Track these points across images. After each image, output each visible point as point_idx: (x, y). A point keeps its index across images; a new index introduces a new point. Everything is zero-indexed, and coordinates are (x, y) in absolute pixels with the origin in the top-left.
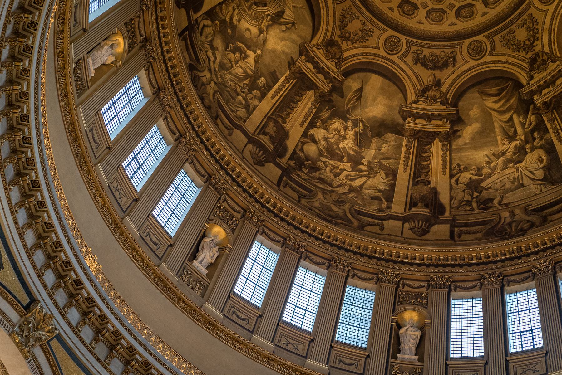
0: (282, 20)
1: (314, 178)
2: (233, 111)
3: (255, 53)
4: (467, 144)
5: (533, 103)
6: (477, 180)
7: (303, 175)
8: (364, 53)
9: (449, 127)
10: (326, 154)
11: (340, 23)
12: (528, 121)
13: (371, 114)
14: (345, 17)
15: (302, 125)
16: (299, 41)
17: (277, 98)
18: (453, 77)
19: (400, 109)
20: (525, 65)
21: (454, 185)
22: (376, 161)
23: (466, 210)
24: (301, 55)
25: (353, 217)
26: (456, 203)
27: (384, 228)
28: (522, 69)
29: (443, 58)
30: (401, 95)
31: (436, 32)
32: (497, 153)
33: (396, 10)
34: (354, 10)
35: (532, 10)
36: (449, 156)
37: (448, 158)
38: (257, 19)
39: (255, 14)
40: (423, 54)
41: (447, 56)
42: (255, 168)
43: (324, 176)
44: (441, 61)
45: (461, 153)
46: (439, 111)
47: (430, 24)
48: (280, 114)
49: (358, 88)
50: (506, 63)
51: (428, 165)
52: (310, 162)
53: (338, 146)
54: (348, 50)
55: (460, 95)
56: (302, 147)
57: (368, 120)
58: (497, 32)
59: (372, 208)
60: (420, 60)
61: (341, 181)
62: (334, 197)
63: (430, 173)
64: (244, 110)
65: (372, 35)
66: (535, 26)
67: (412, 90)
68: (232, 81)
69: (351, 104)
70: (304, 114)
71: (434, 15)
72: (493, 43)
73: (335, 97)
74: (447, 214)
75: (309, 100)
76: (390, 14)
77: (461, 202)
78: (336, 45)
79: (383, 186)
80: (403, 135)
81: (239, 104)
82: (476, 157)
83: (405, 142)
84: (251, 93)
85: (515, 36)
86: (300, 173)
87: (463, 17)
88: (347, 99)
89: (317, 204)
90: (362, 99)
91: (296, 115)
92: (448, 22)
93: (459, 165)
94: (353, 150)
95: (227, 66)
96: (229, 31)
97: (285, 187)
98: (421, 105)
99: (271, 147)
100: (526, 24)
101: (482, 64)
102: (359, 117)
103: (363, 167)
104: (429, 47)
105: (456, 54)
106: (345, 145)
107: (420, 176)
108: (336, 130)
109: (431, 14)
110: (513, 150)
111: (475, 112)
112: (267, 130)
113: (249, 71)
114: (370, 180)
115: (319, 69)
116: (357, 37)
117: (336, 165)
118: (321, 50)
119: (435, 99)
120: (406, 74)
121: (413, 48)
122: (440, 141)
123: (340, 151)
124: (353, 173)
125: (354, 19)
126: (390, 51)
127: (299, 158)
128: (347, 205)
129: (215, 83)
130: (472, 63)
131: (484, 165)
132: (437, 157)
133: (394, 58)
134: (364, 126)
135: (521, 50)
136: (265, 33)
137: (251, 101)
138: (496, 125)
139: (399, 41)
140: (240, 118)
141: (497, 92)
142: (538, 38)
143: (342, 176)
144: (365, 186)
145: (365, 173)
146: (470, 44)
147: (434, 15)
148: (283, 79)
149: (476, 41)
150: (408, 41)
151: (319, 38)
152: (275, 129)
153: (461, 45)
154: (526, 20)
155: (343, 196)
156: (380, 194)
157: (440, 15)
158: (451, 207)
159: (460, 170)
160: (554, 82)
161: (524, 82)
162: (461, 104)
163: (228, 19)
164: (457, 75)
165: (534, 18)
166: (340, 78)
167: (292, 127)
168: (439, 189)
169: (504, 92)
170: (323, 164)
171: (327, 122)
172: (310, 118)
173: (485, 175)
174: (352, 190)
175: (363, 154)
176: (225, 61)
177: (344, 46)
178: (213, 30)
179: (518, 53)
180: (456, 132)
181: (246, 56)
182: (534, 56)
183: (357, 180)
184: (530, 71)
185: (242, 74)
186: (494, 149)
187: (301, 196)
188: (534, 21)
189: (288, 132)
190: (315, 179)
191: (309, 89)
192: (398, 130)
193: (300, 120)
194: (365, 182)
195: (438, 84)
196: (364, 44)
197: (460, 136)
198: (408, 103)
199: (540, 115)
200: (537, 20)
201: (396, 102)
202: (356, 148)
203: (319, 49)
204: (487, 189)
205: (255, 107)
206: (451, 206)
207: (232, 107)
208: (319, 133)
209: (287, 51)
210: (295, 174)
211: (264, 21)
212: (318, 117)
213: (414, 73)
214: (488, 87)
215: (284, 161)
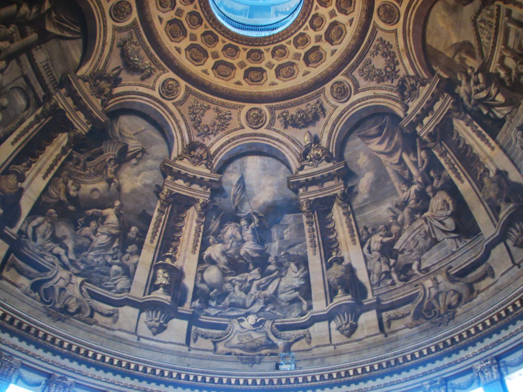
0: (129, 155)
1: (224, 308)
2: (110, 289)
3: (113, 208)
4: (366, 200)
5: (418, 136)
7: (213, 311)
8: (231, 139)
9: (342, 186)
10: (229, 271)
11: (192, 122)
12: (419, 160)
13: (261, 201)
14: (195, 114)
15: (194, 252)
16: (158, 164)
17: (157, 238)
18: (328, 128)
19: (288, 182)
20: (395, 94)
22: (282, 253)
23: (387, 286)
24: (165, 177)
25: (276, 337)
26: (375, 277)
27: (310, 338)
28: (393, 100)
29: (311, 111)
30: (284, 167)
31: (293, 87)
32: (400, 204)
33: (243, 82)
34: (201, 102)
36: (353, 220)
37: (353, 223)
38: (99, 173)
39: (94, 170)
40: (290, 115)
41: (314, 108)
42: (156, 341)
43: (235, 299)
44: (310, 116)
45: (363, 212)
47: (284, 81)
48: (167, 254)
49: (238, 179)
51: (335, 238)
52: (215, 290)
53: (239, 254)
54: (212, 144)
55: (342, 145)
56: (202, 277)
57: (260, 209)
58: (354, 67)
59: (293, 318)
61: (253, 297)
62: (252, 319)
63: (340, 247)
64: (124, 278)
65: (231, 118)
66: (389, 50)
67: (294, 157)
68: (97, 256)
69: (238, 199)
70: (192, 237)
71: (284, 71)
74: (370, 296)
75: (192, 219)
76: (239, 88)
77: (380, 274)
78: (198, 146)
79: (297, 282)
80: (301, 211)
81: (115, 276)
82: (380, 213)
83: (305, 219)
84: (124, 253)
85: (373, 67)
86: (207, 311)
87: (313, 62)
88: (232, 196)
90: (247, 188)
92: (301, 73)
93: (366, 228)
94: (256, 251)
95: (85, 245)
96: (71, 208)
97: (195, 340)
98: (308, 170)
100: (379, 50)
101: (352, 104)
102: (250, 211)
103: (271, 267)
104: (292, 105)
105: (322, 103)
106: (245, 249)
108: (233, 236)
109: (281, 70)
110: (414, 197)
111: (363, 160)
112: (158, 282)
113: (114, 232)
114: (283, 279)
115: (191, 180)
116: (216, 127)
117: (244, 279)
118: (185, 160)
119: (318, 158)
120: (281, 142)
121: (278, 113)
122: (339, 204)
123: (243, 259)
124: (263, 280)
125: (205, 111)
126: (256, 125)
127: (203, 291)
128: (268, 324)
129: (77, 275)
130: (342, 107)
131: (391, 221)
132: (342, 225)
133: (263, 130)
134: (259, 217)
135: (385, 78)
136: (116, 180)
137: (128, 263)
138: (389, 170)
139: (260, 111)
140: (122, 291)
141: (377, 132)
142: (397, 62)
143: (253, 289)
144: (279, 290)
145: (276, 273)
146: (332, 87)
147: (283, 71)
148: (156, 214)
149: (337, 83)
150: (270, 108)
151: (177, 148)
152: (166, 275)
154: (378, 46)
155: (261, 314)
157: (289, 69)
158: (372, 286)
159: (368, 234)
161: (401, 114)
162: (346, 154)
163: (63, 197)
164: (331, 124)
165: (385, 41)
166: (216, 177)
167: (184, 260)
168: (354, 265)
169: (385, 130)
170: (229, 284)
172: (200, 239)
173: (395, 234)
176: (80, 242)
177: (207, 142)
178: (49, 223)
179: (383, 83)
180: (351, 189)
181: (104, 218)
182: (401, 83)
183: (270, 286)
184: (403, 100)
185: (107, 240)
186: (395, 199)
189: (182, 268)
190: (226, 309)
191: (188, 207)
193: (190, 247)
195: (316, 140)
196: (227, 130)
197: (357, 193)
198: (294, 172)
200: (389, 43)
202: (259, 248)
203: (183, 159)
205: (136, 266)
206: (371, 284)
207: (109, 285)
209: (148, 182)
210: (204, 315)
211: (109, 169)
213: (288, 137)
214: (367, 128)
215: (187, 308)
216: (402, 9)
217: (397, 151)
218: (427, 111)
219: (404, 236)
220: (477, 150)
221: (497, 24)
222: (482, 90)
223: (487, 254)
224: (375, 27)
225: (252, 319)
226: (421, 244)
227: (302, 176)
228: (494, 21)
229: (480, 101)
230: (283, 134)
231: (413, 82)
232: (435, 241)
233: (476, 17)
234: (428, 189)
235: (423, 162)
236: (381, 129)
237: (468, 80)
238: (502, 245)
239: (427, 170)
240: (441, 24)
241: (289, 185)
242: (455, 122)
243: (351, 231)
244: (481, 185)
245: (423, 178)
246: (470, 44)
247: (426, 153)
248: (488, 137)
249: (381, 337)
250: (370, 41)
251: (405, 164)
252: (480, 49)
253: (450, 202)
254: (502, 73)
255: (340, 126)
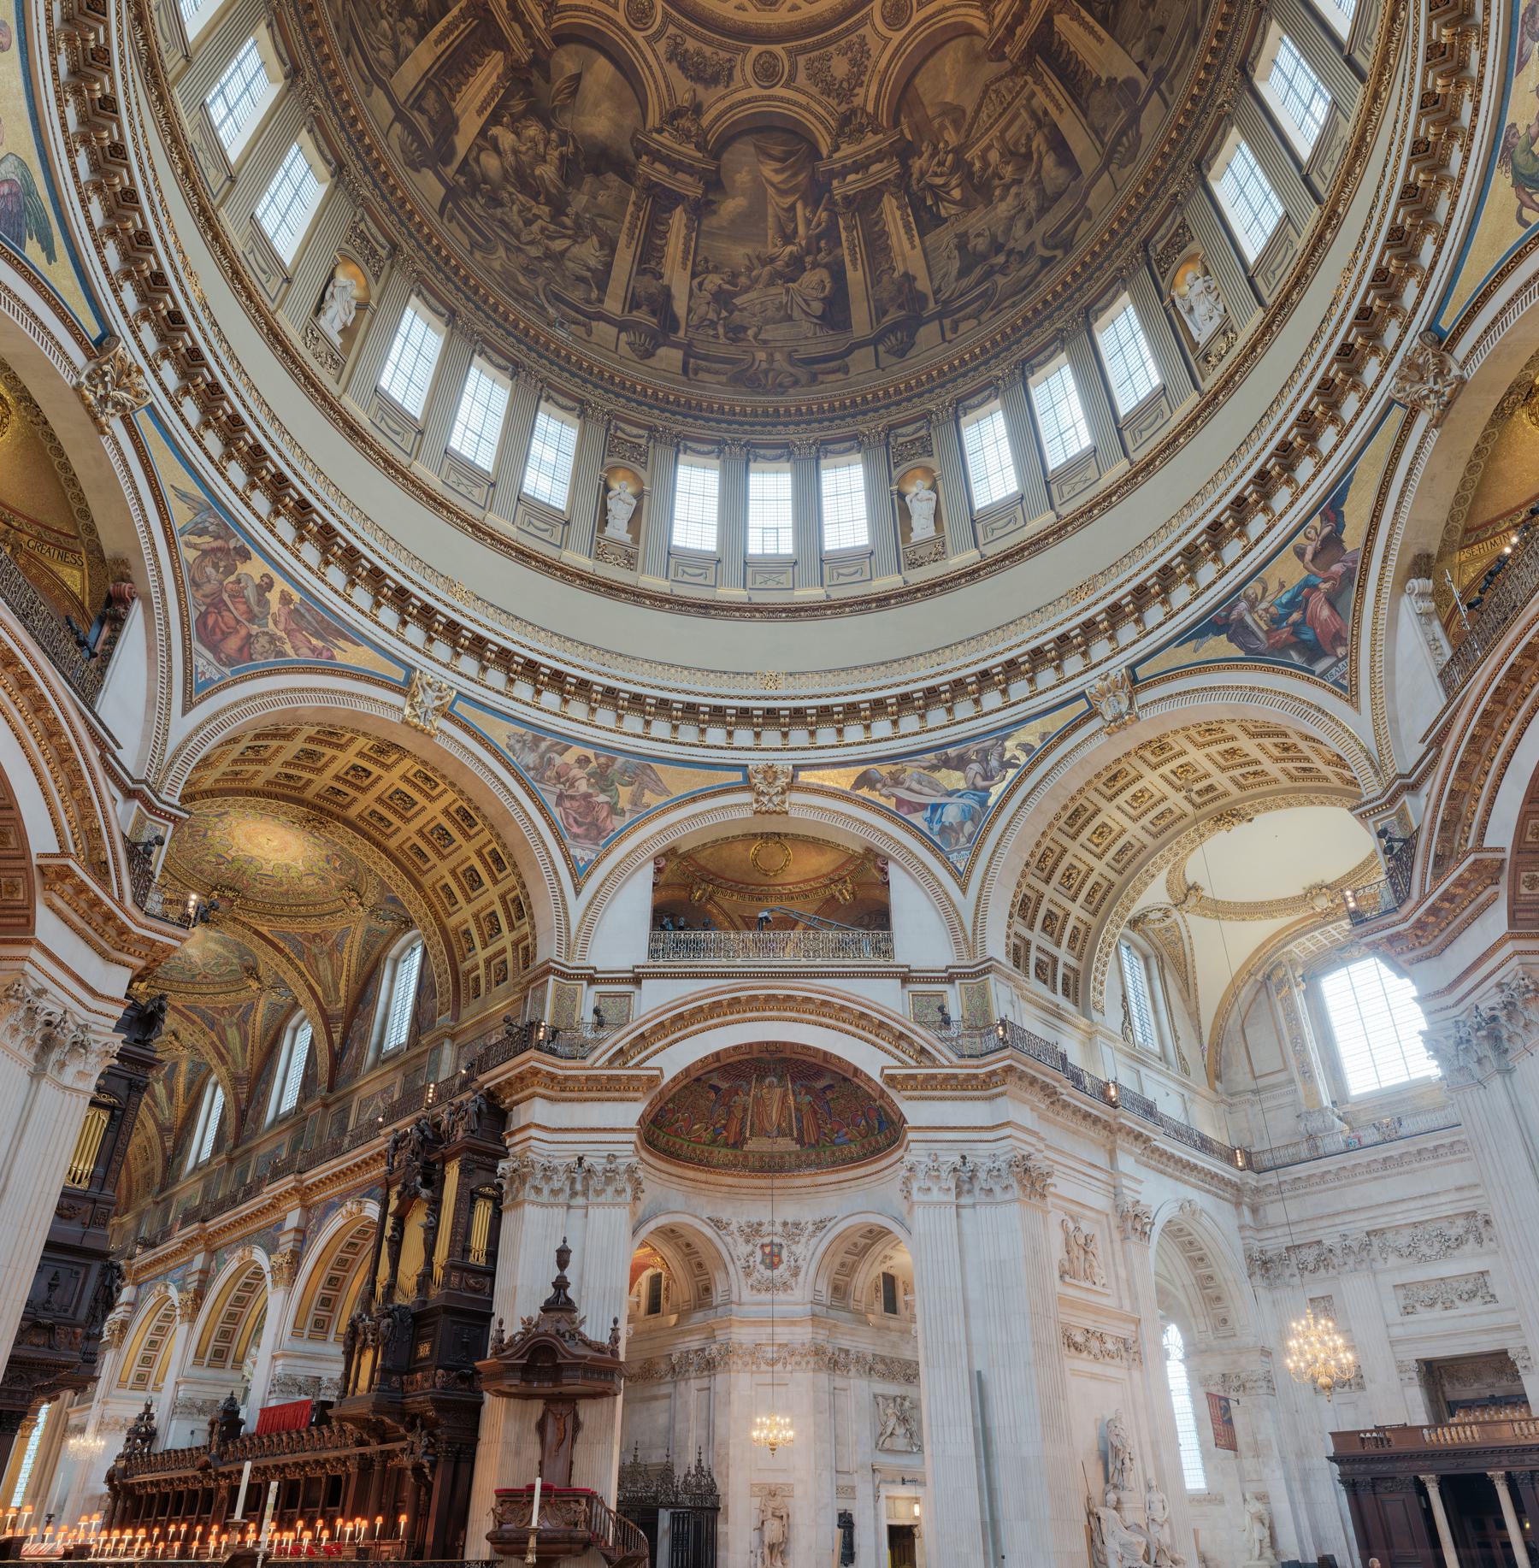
5: (830, 191)
6: (728, 291)
13: (588, 130)
15: (480, 112)
18: (722, 106)
19: (634, 134)
21: (696, 290)
26: (695, 320)
30: (637, 110)
35: (865, 30)
44: (709, 71)
46: (691, 157)
50: (807, 109)
55: (726, 141)
58: (805, 50)
60: (677, 55)
62: (522, 259)
72: (794, 67)
73: (536, 77)
74: (681, 333)
83: (633, 197)
89: (497, 265)
91: (472, 90)
93: (706, 260)
97: (450, 221)
98: (665, 139)
99: (430, 140)
101: (769, 98)
102: (569, 129)
104: (696, 37)
107: (648, 261)
108: (532, 140)
111: (743, 178)
119: (686, 136)
120: (652, 74)
121: (672, 30)
122: (685, 210)
124: (552, 227)
127: (472, 174)
128: (541, 280)
130: (756, 91)
133: (639, 36)
134: (576, 147)
138: (770, 211)
143: (535, 227)
144: (568, 254)
145: (570, 232)
153: (746, 51)
156: (589, 274)
158: (688, 325)
160: (867, 168)
161: (825, 152)
162: (725, 156)
166: (548, 43)
168: (673, 290)
171: (518, 120)
174: (549, 255)
175: (570, 198)
180: (709, 203)
183: (558, 242)
184: (838, 135)
187: (474, 245)
188: (866, 53)
191: (498, 48)
192: (626, 172)
194: (568, 248)
195: (697, 109)
197: (715, 212)
199: (836, 215)
201: (629, 122)
202: (560, 184)
204: (741, 310)
208: (506, 139)
212: (507, 108)
213: (665, 77)
216: (917, 18)
217: (793, 194)
218: (860, 167)
219: (752, 295)
220: (894, 241)
221: (1010, 104)
222: (942, 175)
223: (849, 351)
224: (868, 16)
225: (522, 259)
226: (769, 313)
227: (656, 141)
228: (1009, 99)
229: (931, 187)
230: (662, 68)
231: (865, 121)
232: (790, 318)
233: (992, 83)
234: (809, 259)
235: (819, 225)
236: (789, 154)
237: (932, 156)
238: (872, 348)
239: (819, 237)
240: (947, 69)
241: (633, 138)
242: (885, 198)
243: (686, 252)
244: (876, 281)
245: (808, 244)
246: (964, 112)
247: (829, 217)
248: (915, 232)
249: (684, 378)
250: (849, 31)
251: (795, 215)
252: (971, 126)
253: (828, 286)
254: (978, 165)
255: (740, 113)
